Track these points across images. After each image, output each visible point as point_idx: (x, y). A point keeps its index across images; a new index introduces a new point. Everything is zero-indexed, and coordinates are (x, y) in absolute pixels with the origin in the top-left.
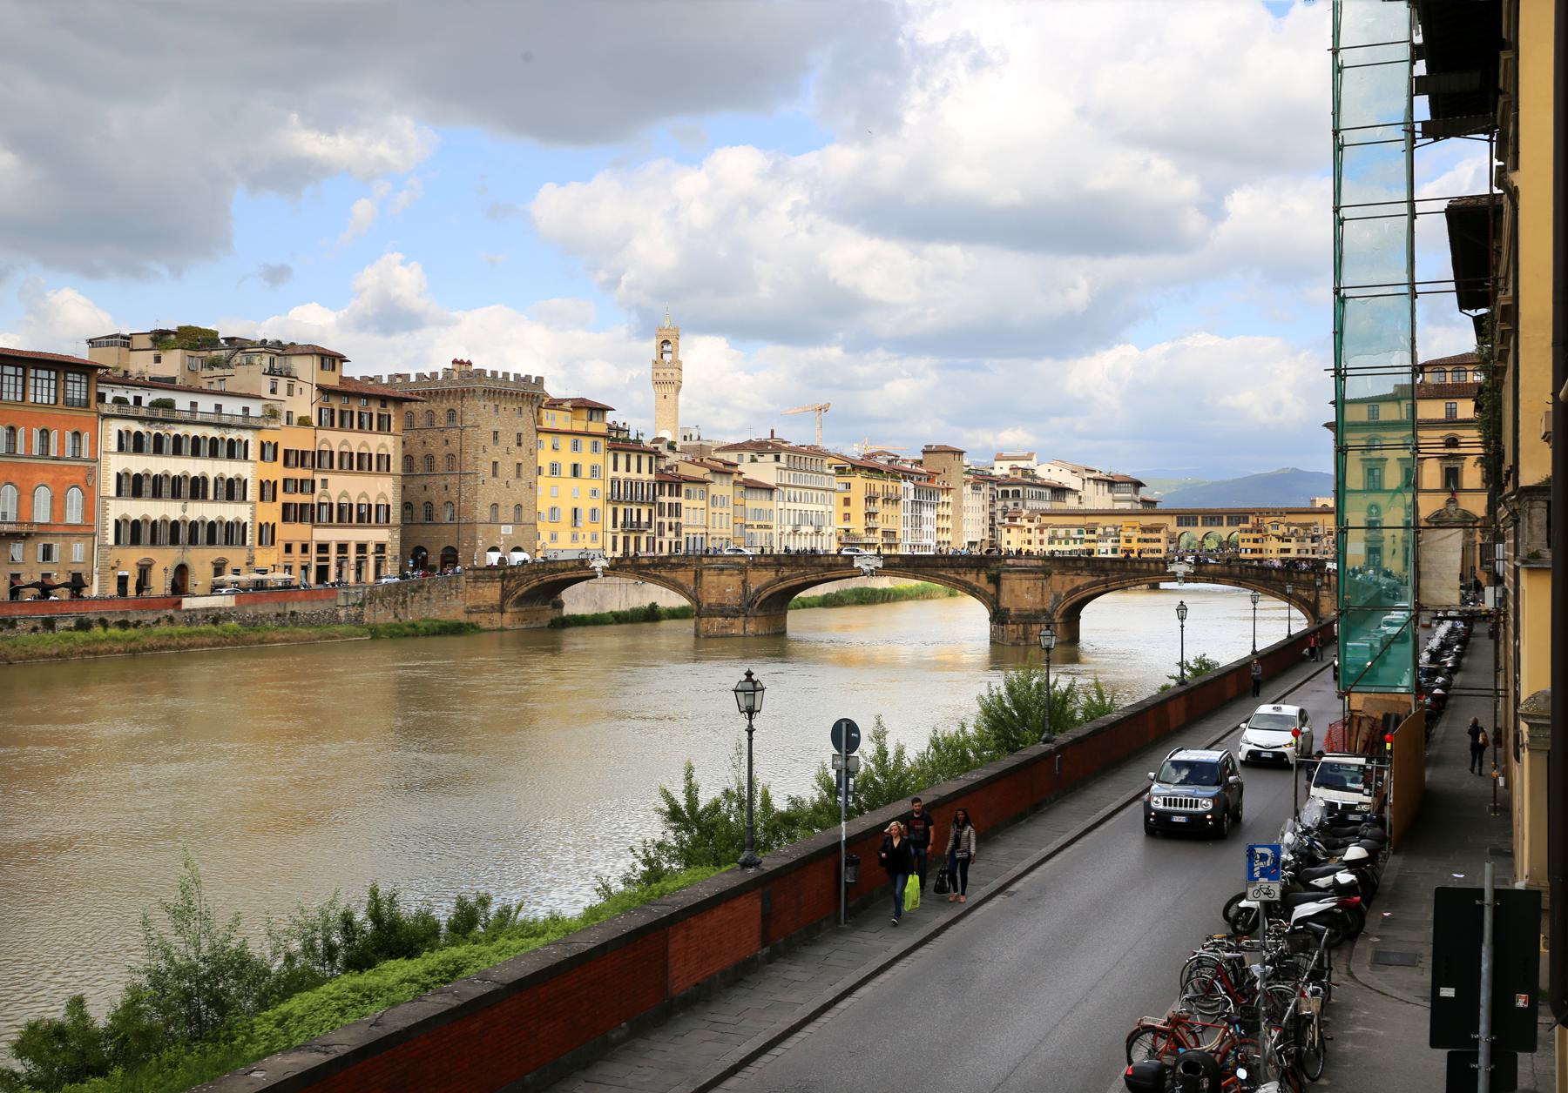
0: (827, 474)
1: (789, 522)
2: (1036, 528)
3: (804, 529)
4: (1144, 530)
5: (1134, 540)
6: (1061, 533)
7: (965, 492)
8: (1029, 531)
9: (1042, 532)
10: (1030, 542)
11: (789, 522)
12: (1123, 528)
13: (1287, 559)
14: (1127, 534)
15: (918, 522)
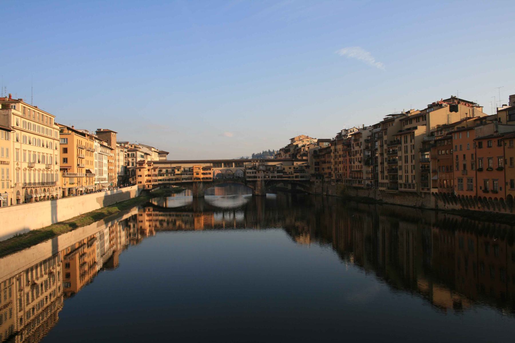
0: (54, 128)
1: (25, 160)
2: (152, 169)
3: (37, 166)
4: (204, 169)
5: (200, 174)
6: (164, 171)
7: (117, 150)
8: (149, 170)
9: (155, 171)
10: (149, 176)
11: (25, 160)
12: (194, 169)
13: (267, 180)
14: (197, 171)
15: (101, 165)
